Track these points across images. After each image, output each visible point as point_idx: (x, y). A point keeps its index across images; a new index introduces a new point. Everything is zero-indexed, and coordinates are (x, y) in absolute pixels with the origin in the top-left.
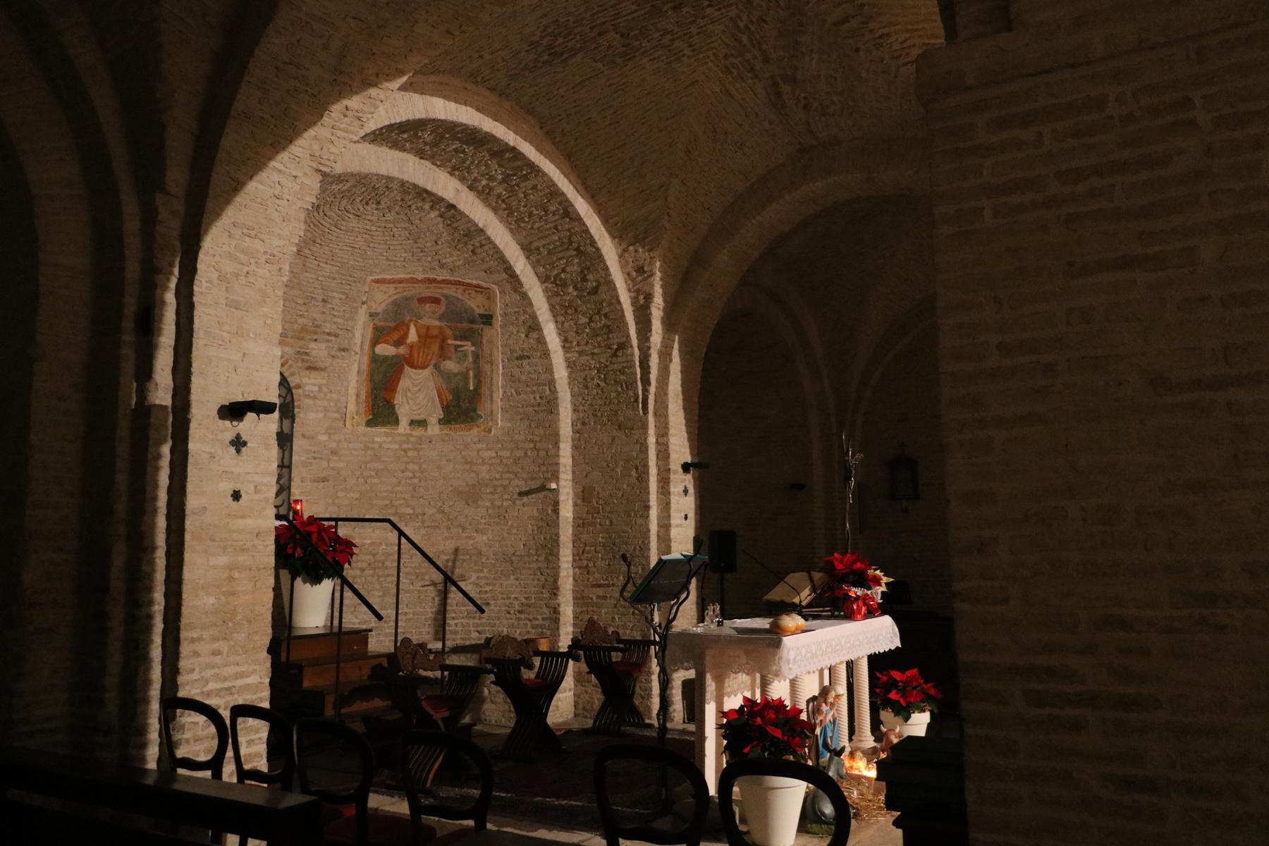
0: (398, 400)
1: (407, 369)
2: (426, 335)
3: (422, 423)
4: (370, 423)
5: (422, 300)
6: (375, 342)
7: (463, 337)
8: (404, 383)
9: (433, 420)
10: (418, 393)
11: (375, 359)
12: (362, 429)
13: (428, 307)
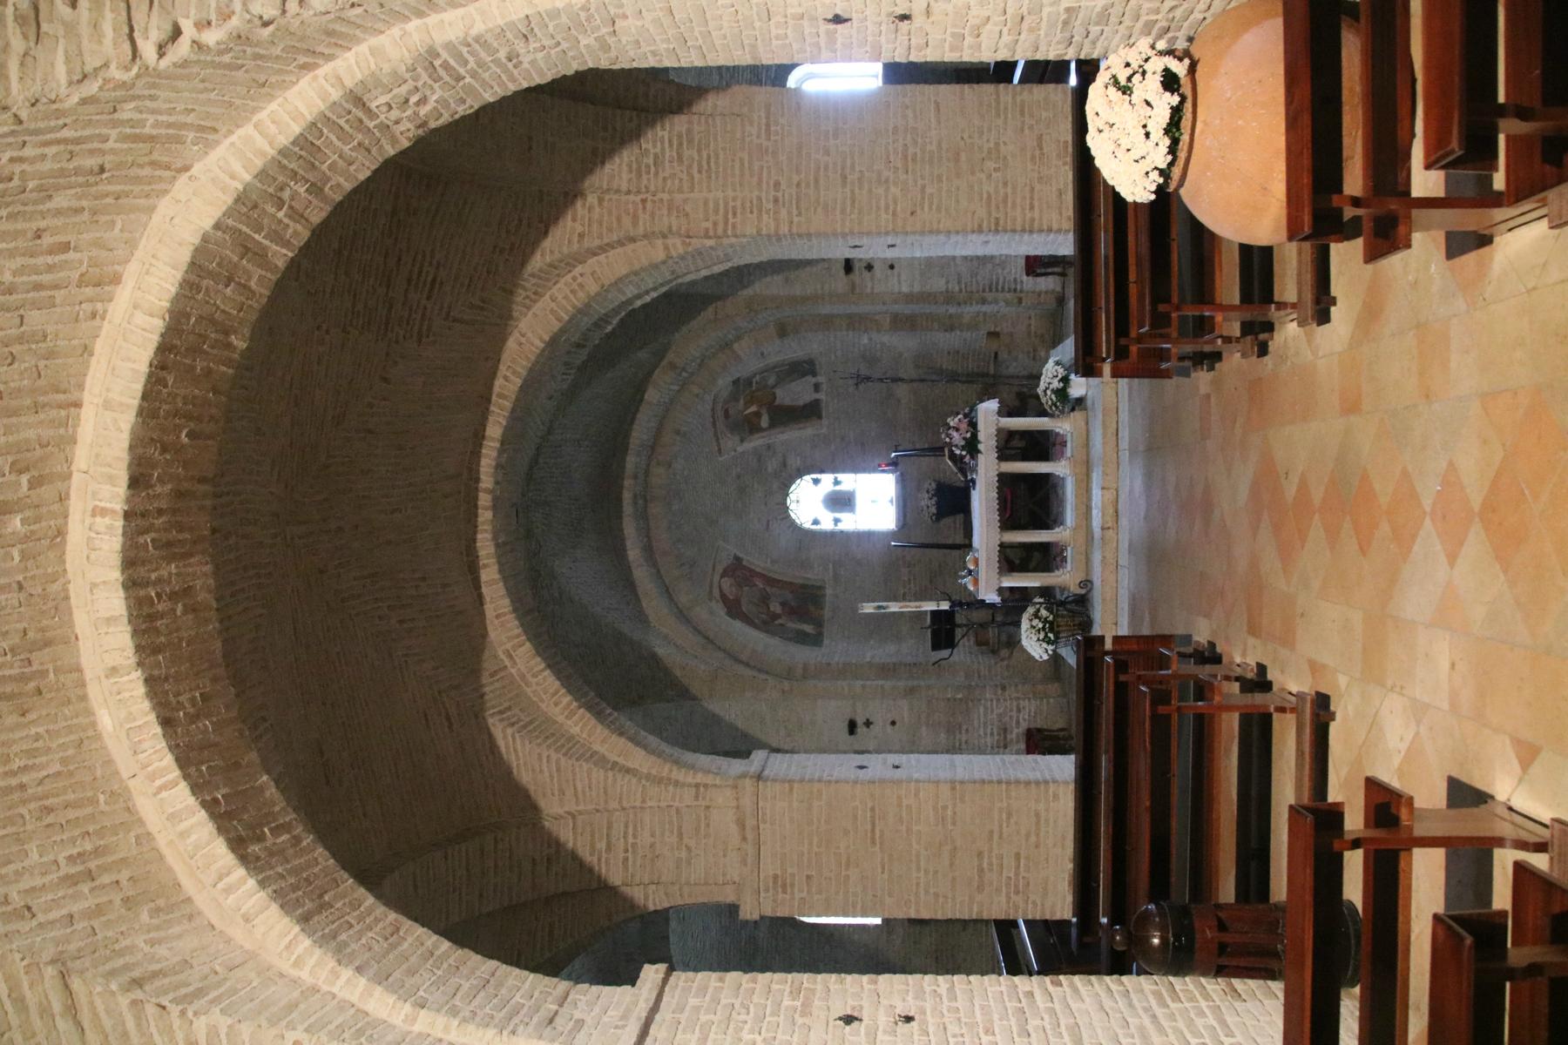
0: (801, 403)
1: (777, 402)
2: (747, 404)
3: (817, 387)
4: (820, 417)
5: (727, 415)
6: (760, 430)
7: (750, 384)
8: (787, 402)
9: (814, 380)
10: (796, 393)
11: (772, 425)
12: (825, 422)
13: (731, 412)
